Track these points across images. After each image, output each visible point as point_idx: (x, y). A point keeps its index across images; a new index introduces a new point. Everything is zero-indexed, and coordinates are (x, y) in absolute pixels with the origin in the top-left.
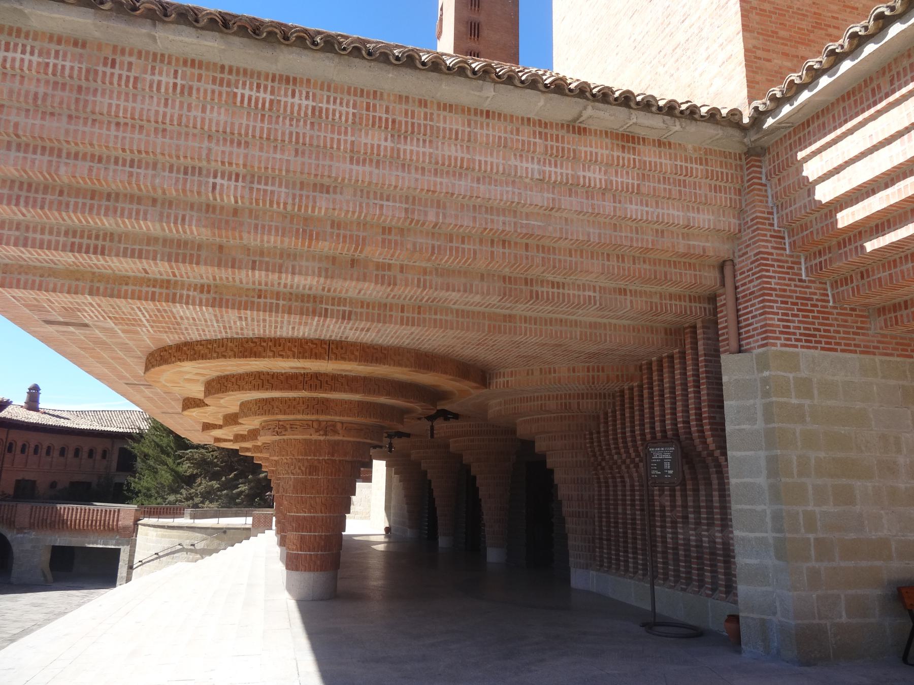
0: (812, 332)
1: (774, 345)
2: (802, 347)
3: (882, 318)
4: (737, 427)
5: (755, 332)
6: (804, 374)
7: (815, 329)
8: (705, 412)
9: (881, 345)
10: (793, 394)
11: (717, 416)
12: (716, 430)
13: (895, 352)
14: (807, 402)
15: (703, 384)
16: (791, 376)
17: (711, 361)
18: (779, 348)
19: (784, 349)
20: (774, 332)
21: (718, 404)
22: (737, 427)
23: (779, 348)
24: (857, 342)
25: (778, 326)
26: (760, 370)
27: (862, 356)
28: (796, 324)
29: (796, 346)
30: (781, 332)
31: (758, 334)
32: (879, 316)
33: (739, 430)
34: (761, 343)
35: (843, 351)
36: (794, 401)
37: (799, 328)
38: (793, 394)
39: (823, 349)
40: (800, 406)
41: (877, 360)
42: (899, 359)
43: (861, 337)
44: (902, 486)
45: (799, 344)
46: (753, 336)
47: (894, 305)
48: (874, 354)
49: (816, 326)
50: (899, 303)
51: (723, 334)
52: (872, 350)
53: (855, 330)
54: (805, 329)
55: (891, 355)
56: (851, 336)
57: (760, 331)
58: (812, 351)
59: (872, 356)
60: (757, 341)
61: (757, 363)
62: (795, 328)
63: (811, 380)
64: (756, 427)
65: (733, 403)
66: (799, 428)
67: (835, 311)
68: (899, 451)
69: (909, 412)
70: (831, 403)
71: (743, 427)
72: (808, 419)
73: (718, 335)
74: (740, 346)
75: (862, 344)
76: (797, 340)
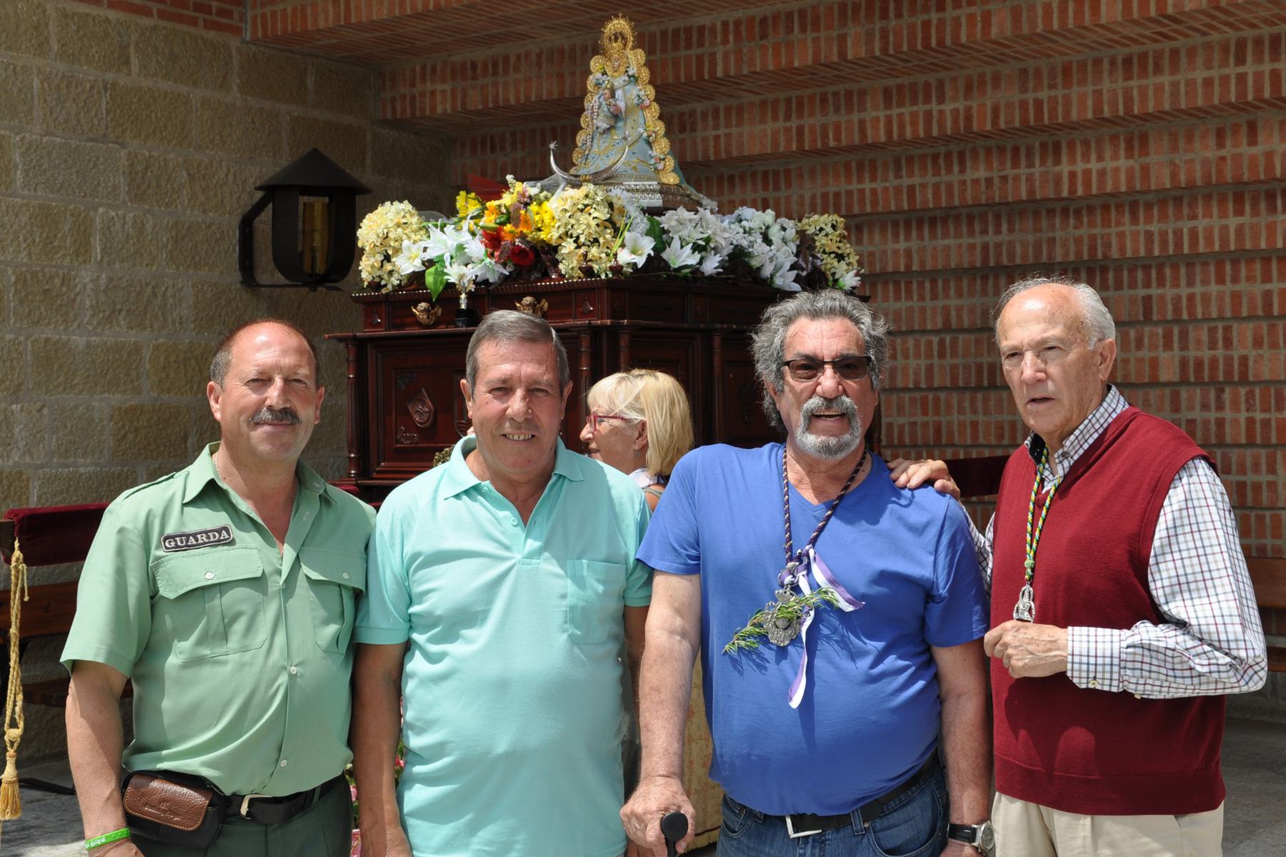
44: (79, 341)
68: (82, 248)
69: (123, 153)
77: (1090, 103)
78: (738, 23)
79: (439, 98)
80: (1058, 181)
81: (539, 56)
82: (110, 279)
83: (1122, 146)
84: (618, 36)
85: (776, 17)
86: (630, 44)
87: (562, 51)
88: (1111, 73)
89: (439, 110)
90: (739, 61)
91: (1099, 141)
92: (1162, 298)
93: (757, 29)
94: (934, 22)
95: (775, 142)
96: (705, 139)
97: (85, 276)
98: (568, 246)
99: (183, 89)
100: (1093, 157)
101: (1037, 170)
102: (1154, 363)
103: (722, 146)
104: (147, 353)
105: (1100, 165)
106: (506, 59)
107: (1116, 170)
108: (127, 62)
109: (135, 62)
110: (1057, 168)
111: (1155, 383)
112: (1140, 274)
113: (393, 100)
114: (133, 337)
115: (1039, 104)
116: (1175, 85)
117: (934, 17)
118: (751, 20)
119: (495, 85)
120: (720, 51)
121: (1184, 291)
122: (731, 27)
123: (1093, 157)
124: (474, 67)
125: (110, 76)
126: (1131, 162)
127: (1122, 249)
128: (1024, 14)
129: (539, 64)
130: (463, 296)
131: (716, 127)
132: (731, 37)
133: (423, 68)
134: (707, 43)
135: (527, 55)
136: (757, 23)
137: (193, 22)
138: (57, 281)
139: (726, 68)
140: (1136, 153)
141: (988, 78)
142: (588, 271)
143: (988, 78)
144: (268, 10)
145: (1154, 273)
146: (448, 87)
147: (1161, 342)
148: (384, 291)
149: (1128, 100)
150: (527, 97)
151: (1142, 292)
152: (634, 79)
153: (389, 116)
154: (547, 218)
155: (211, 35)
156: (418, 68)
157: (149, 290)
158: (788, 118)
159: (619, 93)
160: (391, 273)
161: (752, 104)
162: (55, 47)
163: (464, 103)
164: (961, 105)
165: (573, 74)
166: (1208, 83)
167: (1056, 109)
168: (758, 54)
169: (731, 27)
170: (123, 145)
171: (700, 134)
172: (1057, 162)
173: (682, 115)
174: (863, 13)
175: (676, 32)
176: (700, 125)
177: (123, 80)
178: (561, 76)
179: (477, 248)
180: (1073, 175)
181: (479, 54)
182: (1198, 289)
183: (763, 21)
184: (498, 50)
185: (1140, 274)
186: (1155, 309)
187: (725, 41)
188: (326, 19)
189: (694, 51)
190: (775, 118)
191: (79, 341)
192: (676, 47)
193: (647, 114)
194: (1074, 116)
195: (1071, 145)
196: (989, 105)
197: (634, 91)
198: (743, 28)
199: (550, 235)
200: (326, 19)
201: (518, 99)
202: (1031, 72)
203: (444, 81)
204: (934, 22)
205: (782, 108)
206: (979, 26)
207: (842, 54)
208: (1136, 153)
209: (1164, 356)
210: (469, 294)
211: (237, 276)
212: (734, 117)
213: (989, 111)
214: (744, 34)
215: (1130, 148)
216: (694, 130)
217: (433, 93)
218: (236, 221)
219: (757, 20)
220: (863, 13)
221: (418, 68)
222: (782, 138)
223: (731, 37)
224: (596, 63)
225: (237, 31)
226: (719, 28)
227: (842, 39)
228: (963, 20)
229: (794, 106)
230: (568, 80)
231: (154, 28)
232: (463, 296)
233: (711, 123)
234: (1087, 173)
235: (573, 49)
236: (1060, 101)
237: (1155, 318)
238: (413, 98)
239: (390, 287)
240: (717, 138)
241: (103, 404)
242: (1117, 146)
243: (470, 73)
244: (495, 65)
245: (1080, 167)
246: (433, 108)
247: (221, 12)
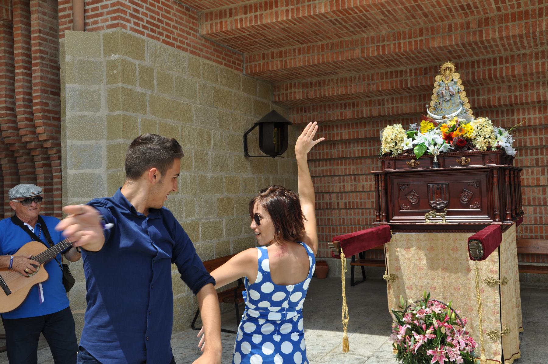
0: (156, 23)
1: (125, 27)
2: (148, 35)
3: (209, 23)
4: (79, 114)
5: (105, 10)
6: (148, 63)
7: (159, 20)
8: (37, 97)
9: (204, 49)
10: (138, 82)
11: (50, 102)
12: (48, 118)
13: (213, 58)
14: (148, 92)
15: (36, 65)
16: (137, 62)
17: (45, 40)
18: (129, 32)
19: (133, 33)
20: (125, 13)
21: (55, 89)
22: (79, 114)
23: (129, 32)
24: (188, 41)
25: (129, 8)
26: (109, 51)
27: (191, 56)
28: (144, 11)
29: (143, 33)
30: (131, 15)
31: (108, 13)
32: (207, 21)
33: (81, 117)
34: (110, 22)
35: (179, 47)
36: (138, 89)
37: (146, 15)
38: (138, 82)
39: (164, 41)
40: (143, 95)
41: (200, 61)
42: (215, 64)
43: (192, 37)
44: (209, 176)
45: (146, 31)
46: (101, 15)
47: (221, 12)
48: (199, 56)
49: (160, 17)
50: (225, 11)
51: (64, 9)
52: (198, 51)
53: (188, 29)
54: (152, 17)
55: (210, 59)
56: (185, 35)
57: (110, 9)
58: (155, 41)
59: (198, 58)
60: (106, 20)
61: (105, 45)
62: (143, 14)
63: (152, 70)
64: (99, 114)
65: (76, 86)
66: (140, 117)
67: (175, 7)
69: (217, 111)
70: (166, 96)
71: (85, 113)
72: (148, 109)
73: (56, 11)
74: (85, 24)
75: (192, 44)
76: (144, 27)
77: (535, 96)
78: (416, 70)
79: (297, 94)
81: (337, 80)
82: (215, 154)
83: (537, 110)
85: (431, 68)
86: (453, 71)
87: (346, 79)
88: (543, 86)
89: (297, 98)
90: (416, 82)
91: (528, 109)
92: (542, 159)
93: (423, 72)
94: (493, 69)
95: (415, 109)
96: (388, 108)
97: (210, 153)
98: (480, 139)
99: (230, 90)
100: (526, 114)
101: (505, 118)
102: (538, 179)
103: (395, 110)
104: (224, 179)
105: (529, 116)
106: (324, 81)
107: (535, 118)
108: (218, 80)
109: (219, 80)
110: (513, 117)
111: (538, 186)
112: (534, 151)
113: (279, 95)
114: (221, 174)
115: (516, 97)
117: (493, 67)
118: (421, 68)
119: (320, 90)
120: (409, 79)
122: (413, 71)
123: (526, 114)
124: (311, 84)
125: (214, 85)
126: (540, 115)
127: (531, 143)
128: (528, 66)
129: (337, 83)
130: (435, 157)
131: (392, 104)
132: (413, 74)
133: (291, 84)
134: (404, 76)
135: (332, 80)
136: (423, 69)
137: (232, 67)
138: (203, 155)
139: (411, 84)
140: (542, 112)
141: (496, 88)
142: (489, 148)
143: (496, 88)
144: (253, 64)
145: (539, 151)
146: (301, 90)
147: (540, 172)
148: (393, 156)
150: (333, 94)
151: (535, 157)
152: (455, 83)
153: (277, 100)
154: (469, 129)
155: (236, 72)
156: (289, 84)
157: (224, 158)
158: (420, 101)
159: (450, 88)
160: (397, 149)
161: (406, 97)
162: (202, 74)
163: (307, 96)
164: (486, 97)
165: (351, 86)
167: (522, 98)
168: (424, 79)
169: (413, 71)
170: (217, 108)
171: (386, 106)
172: (513, 115)
173: (379, 100)
174: (464, 67)
175: (391, 72)
176: (386, 103)
177: (217, 87)
178: (346, 87)
179: (440, 140)
181: (314, 80)
183: (426, 69)
184: (321, 78)
185: (534, 151)
186: (540, 162)
187: (411, 75)
188: (277, 67)
189: (399, 79)
190: (415, 101)
191: (209, 176)
192: (391, 77)
193: (461, 95)
196: (497, 96)
197: (456, 87)
198: (418, 71)
199: (472, 135)
200: (277, 67)
201: (329, 94)
202: (512, 86)
203: (299, 88)
204: (493, 69)
205: (418, 98)
206: (510, 70)
208: (542, 112)
209: (542, 177)
210: (438, 157)
211: (243, 154)
212: (399, 101)
213: (497, 99)
214: (418, 73)
216: (384, 104)
217: (295, 93)
218: (243, 135)
219: (423, 68)
220: (464, 67)
221: (289, 84)
222: (418, 108)
223: (413, 74)
224: (438, 78)
225: (241, 71)
226: (408, 71)
228: (504, 69)
229: (422, 98)
230: (349, 88)
231: (223, 69)
232: (435, 157)
233: (390, 102)
235: (351, 78)
236: (524, 95)
237: (540, 165)
238: (287, 94)
239: (396, 154)
240: (393, 108)
241: (215, 197)
242: (535, 110)
243: (309, 86)
244: (320, 83)
246: (295, 98)
247: (239, 65)
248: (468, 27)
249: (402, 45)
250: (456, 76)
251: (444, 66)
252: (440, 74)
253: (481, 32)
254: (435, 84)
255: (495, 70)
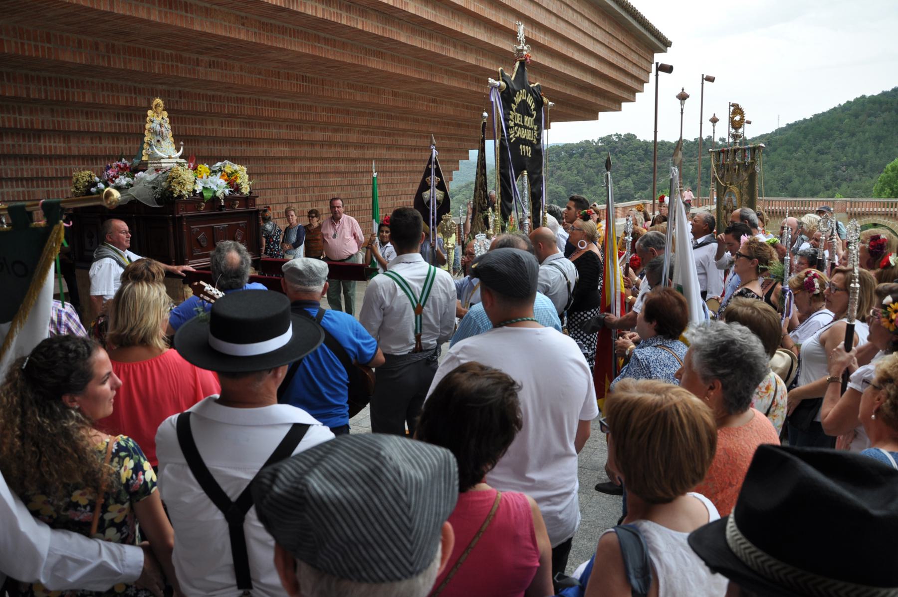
80: (40, 148)
84: (157, 105)
101: (32, 143)
116: (102, 124)
117: (65, 90)
121: (60, 189)
127: (48, 173)
149: (88, 126)
151: (46, 189)
166: (111, 125)
172: (40, 141)
180: (45, 147)
182: (64, 188)
194: (71, 129)
195: (45, 137)
207: (28, 95)
215: (64, 140)
227: (28, 89)
234: (50, 147)
245: (48, 144)
248: (97, 49)
249: (26, 47)
250: (165, 114)
251: (155, 103)
252: (151, 109)
253: (109, 57)
254: (148, 119)
255: (68, 93)
